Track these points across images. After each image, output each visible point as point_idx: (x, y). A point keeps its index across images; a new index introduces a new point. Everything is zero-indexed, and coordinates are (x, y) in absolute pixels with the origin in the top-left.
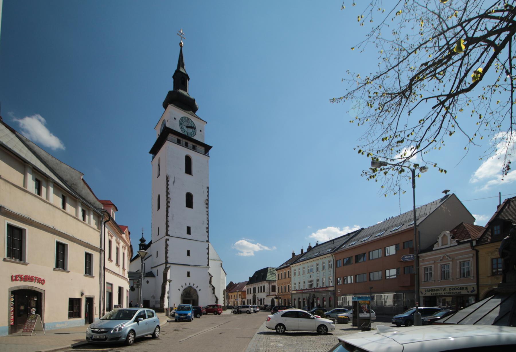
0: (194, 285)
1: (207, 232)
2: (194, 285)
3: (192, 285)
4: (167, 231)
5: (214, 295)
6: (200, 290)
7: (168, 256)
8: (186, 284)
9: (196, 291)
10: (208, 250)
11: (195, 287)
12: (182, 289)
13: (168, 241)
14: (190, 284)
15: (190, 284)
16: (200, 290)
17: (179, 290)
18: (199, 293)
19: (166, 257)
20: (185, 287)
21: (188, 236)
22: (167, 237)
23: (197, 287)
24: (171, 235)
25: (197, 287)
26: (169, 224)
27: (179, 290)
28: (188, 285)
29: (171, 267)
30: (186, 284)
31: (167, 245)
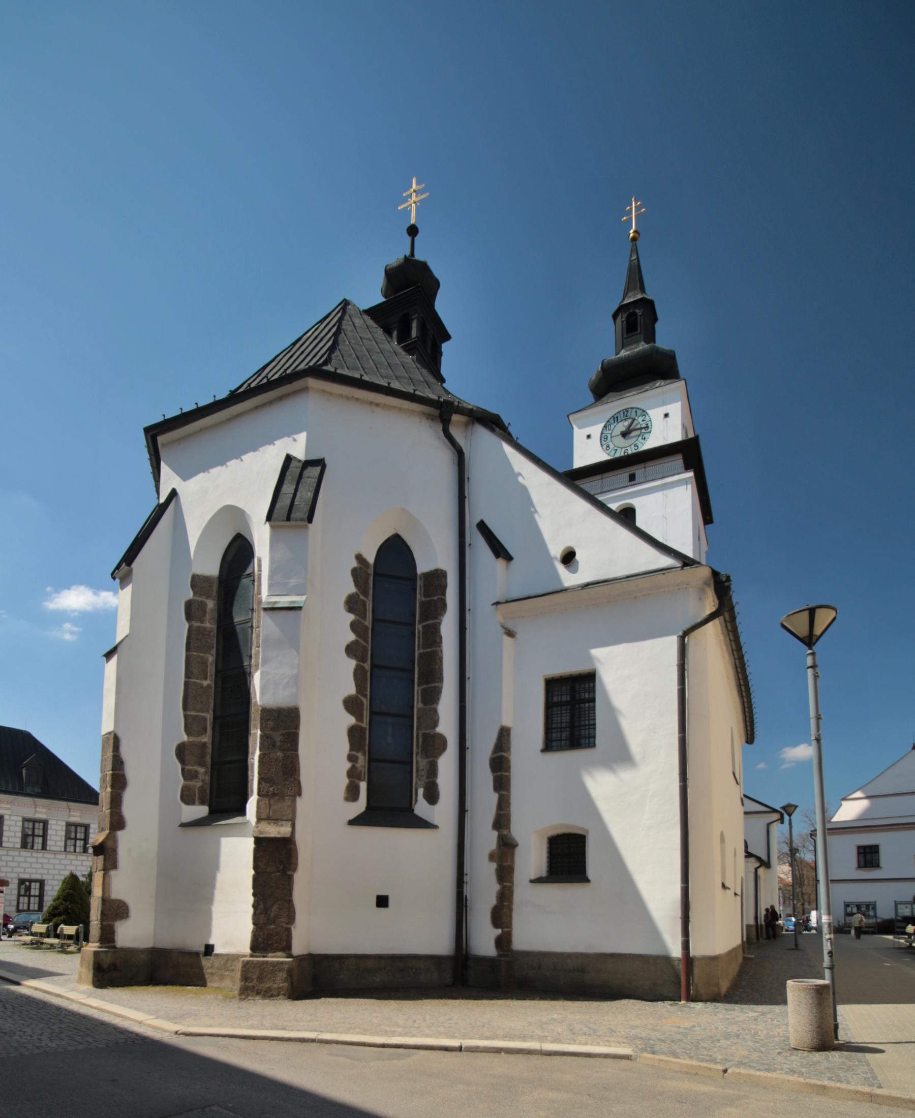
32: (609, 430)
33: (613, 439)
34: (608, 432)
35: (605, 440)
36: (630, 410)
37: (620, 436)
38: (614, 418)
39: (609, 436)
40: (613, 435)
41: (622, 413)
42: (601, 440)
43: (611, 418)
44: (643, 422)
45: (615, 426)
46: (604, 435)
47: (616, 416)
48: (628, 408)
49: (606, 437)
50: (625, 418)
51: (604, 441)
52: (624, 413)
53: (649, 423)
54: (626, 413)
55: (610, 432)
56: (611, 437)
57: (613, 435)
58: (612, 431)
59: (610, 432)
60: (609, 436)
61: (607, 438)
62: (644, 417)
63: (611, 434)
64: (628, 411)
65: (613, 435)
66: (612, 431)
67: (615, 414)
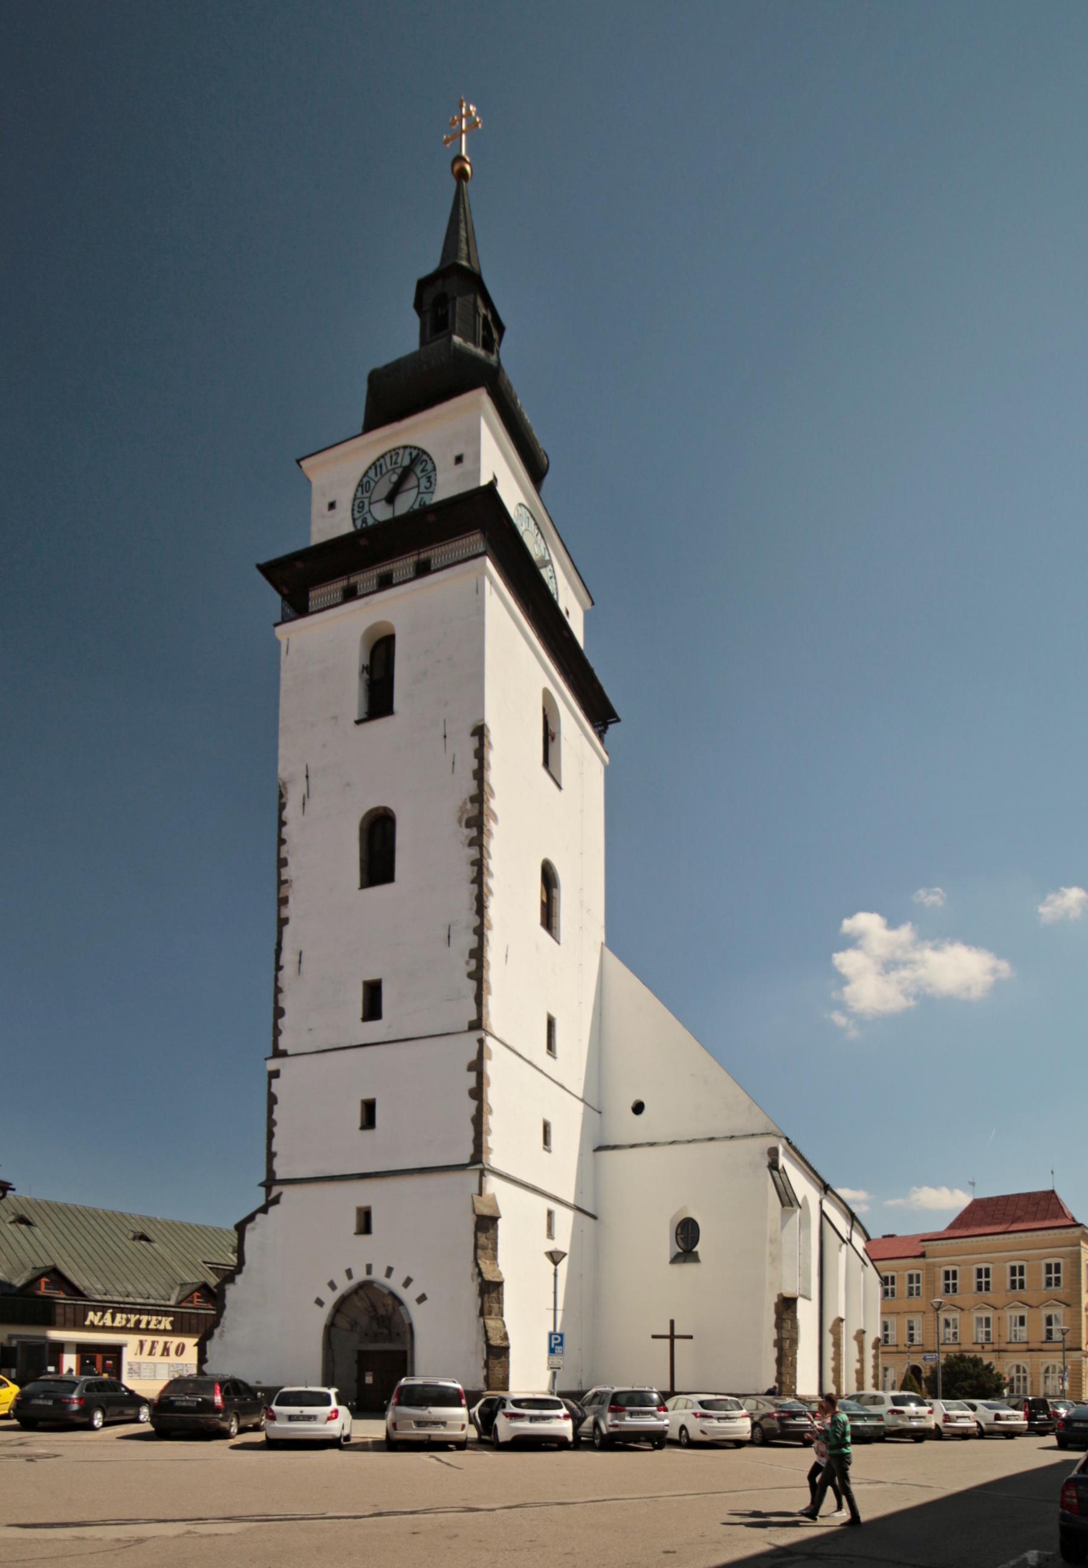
0: (389, 1271)
1: (470, 976)
2: (389, 1271)
3: (378, 1275)
4: (277, 1032)
5: (481, 1320)
6: (422, 1299)
7: (274, 1148)
8: (349, 1274)
9: (398, 1301)
10: (473, 1075)
11: (395, 1284)
12: (331, 1298)
13: (274, 1081)
14: (369, 1269)
15: (369, 1269)
16: (422, 1299)
17: (319, 1302)
18: (419, 1316)
19: (271, 1156)
20: (344, 1285)
21: (375, 1030)
22: (273, 1065)
23: (408, 1282)
24: (289, 1052)
25: (408, 1282)
26: (285, 1002)
27: (319, 1302)
28: (360, 1276)
29: (283, 1199)
30: (349, 1274)
31: (272, 1100)
32: (367, 492)
33: (372, 507)
34: (366, 495)
35: (360, 510)
36: (401, 452)
37: (383, 502)
38: (376, 468)
39: (366, 501)
40: (373, 500)
41: (388, 456)
42: (353, 510)
43: (370, 468)
44: (423, 474)
45: (376, 483)
46: (358, 501)
47: (378, 464)
48: (399, 448)
49: (361, 505)
50: (393, 466)
51: (359, 512)
52: (391, 457)
53: (432, 474)
54: (394, 458)
55: (368, 495)
56: (370, 504)
57: (372, 501)
58: (371, 494)
59: (368, 495)
60: (366, 501)
61: (363, 507)
62: (424, 463)
63: (370, 498)
64: (398, 454)
65: (372, 501)
66: (371, 494)
67: (378, 460)
